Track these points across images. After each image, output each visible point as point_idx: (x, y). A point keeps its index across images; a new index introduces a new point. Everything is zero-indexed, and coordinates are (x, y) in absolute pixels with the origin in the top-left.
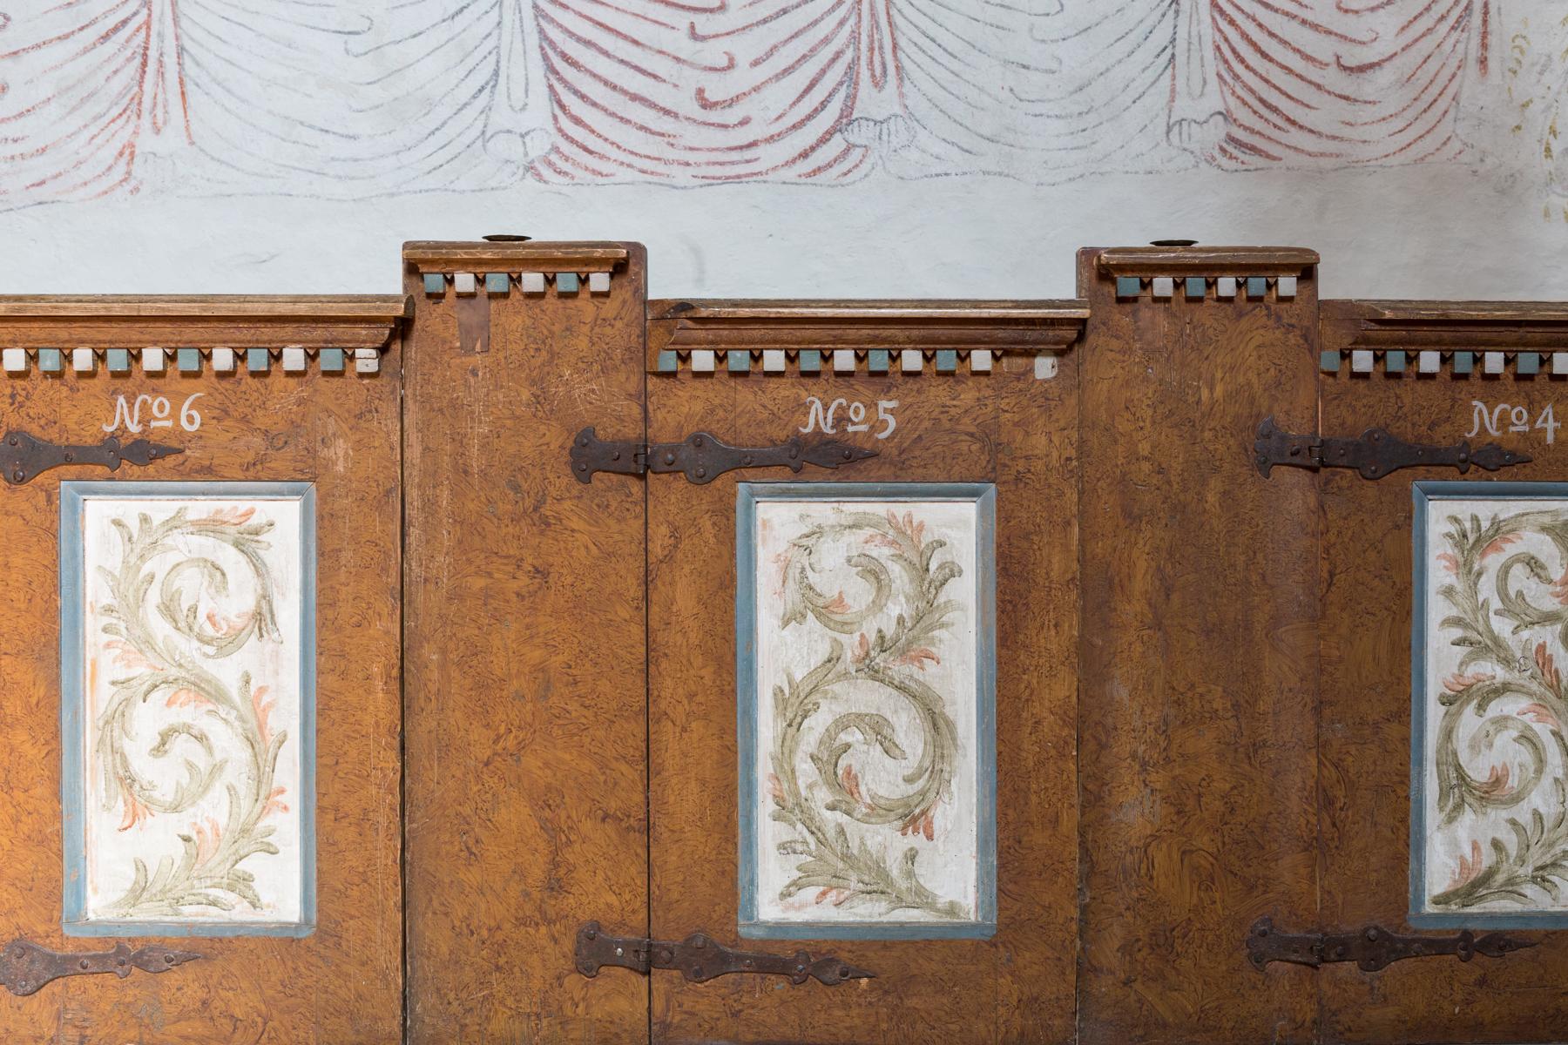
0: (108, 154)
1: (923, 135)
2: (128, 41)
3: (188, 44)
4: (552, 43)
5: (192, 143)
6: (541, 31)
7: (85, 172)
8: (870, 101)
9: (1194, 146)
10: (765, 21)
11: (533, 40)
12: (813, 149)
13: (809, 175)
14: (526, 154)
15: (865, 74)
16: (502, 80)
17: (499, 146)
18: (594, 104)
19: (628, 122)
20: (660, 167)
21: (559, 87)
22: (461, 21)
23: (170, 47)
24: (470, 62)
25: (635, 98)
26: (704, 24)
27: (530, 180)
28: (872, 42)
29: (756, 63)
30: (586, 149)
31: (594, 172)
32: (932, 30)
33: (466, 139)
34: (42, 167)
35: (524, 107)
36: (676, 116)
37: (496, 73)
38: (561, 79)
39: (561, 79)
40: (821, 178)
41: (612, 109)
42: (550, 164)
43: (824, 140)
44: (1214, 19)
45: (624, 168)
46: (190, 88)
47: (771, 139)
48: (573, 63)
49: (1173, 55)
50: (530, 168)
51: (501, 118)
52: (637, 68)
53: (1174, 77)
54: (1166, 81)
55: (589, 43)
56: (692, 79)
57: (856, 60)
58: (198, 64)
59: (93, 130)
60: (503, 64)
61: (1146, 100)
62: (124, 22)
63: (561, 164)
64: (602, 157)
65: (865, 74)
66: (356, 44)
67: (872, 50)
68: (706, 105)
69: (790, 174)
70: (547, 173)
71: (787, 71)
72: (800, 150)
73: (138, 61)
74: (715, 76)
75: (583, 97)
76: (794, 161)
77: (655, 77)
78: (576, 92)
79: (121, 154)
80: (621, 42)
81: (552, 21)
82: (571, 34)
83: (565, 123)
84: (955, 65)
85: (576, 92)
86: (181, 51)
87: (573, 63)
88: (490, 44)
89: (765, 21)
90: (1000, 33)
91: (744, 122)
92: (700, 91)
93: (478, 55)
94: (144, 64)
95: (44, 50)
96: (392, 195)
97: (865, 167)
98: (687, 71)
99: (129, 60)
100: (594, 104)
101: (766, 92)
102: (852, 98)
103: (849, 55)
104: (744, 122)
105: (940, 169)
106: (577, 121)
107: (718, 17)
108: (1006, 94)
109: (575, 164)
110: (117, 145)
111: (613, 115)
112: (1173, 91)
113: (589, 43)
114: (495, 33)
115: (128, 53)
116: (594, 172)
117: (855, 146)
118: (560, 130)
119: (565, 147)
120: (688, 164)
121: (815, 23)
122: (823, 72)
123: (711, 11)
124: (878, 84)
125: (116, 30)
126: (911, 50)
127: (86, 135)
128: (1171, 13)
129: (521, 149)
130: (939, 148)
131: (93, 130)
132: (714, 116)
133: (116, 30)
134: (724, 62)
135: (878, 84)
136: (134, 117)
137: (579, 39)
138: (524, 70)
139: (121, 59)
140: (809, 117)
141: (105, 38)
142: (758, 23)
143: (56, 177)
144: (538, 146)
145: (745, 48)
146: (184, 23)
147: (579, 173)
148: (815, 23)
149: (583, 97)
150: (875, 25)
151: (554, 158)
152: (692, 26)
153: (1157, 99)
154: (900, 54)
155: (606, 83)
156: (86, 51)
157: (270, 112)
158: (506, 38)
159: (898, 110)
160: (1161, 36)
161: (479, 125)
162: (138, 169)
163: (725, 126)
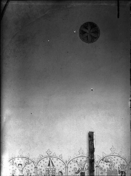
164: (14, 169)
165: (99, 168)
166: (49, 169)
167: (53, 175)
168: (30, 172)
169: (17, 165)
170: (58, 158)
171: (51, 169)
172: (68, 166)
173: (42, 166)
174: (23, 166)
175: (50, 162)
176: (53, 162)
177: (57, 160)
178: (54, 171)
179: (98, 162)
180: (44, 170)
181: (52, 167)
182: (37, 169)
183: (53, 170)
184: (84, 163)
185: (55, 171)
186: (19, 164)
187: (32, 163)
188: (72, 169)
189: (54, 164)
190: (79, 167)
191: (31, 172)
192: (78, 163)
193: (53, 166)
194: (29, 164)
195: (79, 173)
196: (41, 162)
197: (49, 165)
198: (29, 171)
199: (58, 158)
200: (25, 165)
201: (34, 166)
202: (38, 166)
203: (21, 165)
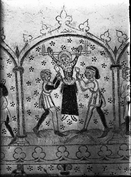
165: (121, 71)
179: (120, 51)
184: (74, 57)
190: (57, 69)
192: (56, 56)
195: (56, 88)
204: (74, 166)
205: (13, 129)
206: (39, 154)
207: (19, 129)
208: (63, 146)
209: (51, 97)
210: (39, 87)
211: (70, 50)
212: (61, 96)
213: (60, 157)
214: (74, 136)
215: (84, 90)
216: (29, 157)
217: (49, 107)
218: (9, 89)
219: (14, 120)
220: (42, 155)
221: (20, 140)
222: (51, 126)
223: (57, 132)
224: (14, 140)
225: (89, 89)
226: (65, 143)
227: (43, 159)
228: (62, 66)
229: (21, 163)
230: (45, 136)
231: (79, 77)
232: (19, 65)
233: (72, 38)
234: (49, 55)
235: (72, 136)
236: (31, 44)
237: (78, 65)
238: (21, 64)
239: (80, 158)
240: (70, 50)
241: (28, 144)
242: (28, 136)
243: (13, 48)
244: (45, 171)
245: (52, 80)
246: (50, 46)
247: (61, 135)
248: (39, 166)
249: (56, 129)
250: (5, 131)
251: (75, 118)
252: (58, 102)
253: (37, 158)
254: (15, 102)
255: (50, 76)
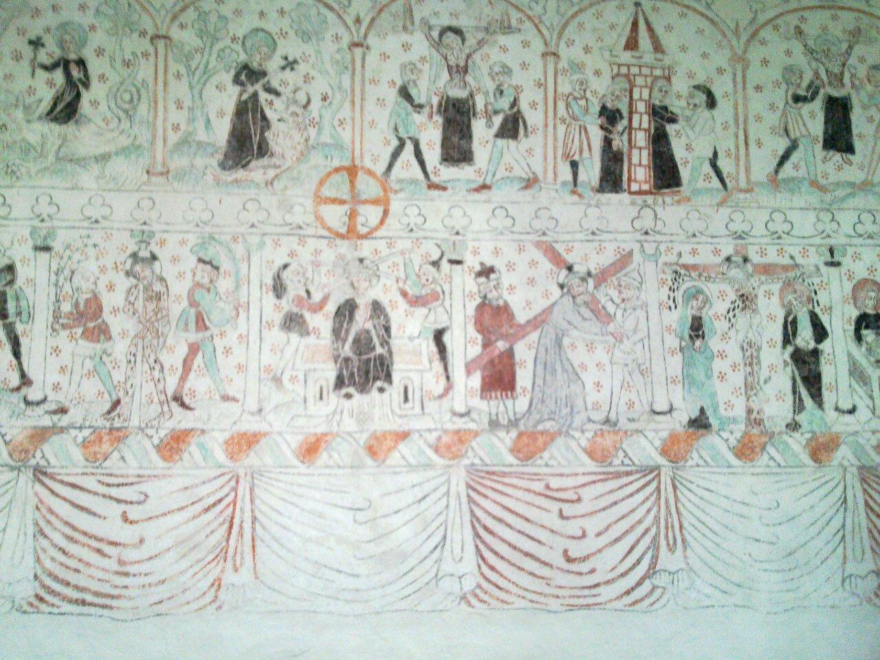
0: (204, 584)
1: (698, 582)
2: (221, 512)
3: (259, 515)
4: (478, 520)
5: (257, 578)
6: (472, 511)
7: (189, 596)
8: (667, 560)
9: (859, 591)
10: (604, 509)
11: (467, 517)
12: (633, 589)
13: (630, 605)
14: (462, 589)
15: (663, 543)
16: (448, 541)
17: (446, 584)
18: (502, 558)
19: (523, 569)
20: (542, 599)
21: (481, 547)
22: (424, 505)
23: (248, 516)
24: (430, 530)
25: (527, 554)
26: (568, 509)
27: (464, 605)
28: (667, 523)
29: (599, 534)
30: (498, 587)
31: (502, 601)
32: (702, 516)
33: (426, 580)
34: (162, 592)
35: (461, 560)
36: (551, 566)
37: (445, 538)
38: (483, 542)
39: (483, 542)
40: (637, 607)
41: (513, 561)
42: (476, 596)
43: (639, 583)
44: (867, 513)
45: (520, 599)
46: (258, 543)
47: (608, 582)
48: (491, 532)
49: (844, 536)
50: (464, 598)
51: (447, 567)
52: (528, 536)
53: (845, 548)
54: (840, 550)
55: (500, 520)
56: (562, 543)
57: (658, 534)
58: (264, 528)
59: (196, 569)
60: (449, 530)
61: (829, 561)
62: (220, 501)
63: (482, 596)
64: (507, 592)
65: (663, 543)
66: (361, 516)
67: (667, 528)
68: (569, 560)
69: (619, 604)
70: (473, 601)
71: (617, 540)
72: (625, 590)
73: (226, 526)
74: (574, 542)
75: (496, 553)
76: (622, 596)
77: (539, 542)
78: (492, 550)
79: (213, 585)
80: (519, 520)
81: (478, 505)
82: (490, 514)
83: (485, 569)
84: (717, 540)
85: (492, 550)
86: (254, 519)
87: (491, 532)
88: (442, 518)
89: (604, 509)
90: (742, 520)
91: (592, 571)
92: (566, 552)
93: (434, 525)
94: (231, 527)
95: (168, 517)
96: (378, 613)
97: (663, 601)
98: (557, 538)
99: (222, 524)
100: (502, 558)
101: (604, 553)
102: (655, 559)
103: (654, 530)
104: (592, 571)
105: (708, 602)
106: (492, 568)
107: (577, 506)
108: (745, 558)
109: (490, 595)
110: (210, 579)
111: (514, 565)
112: (845, 557)
113: (500, 520)
114: (444, 514)
115: (221, 519)
116: (502, 601)
117: (657, 587)
118: (482, 574)
119: (485, 585)
120: (558, 597)
121: (633, 511)
122: (638, 541)
123: (572, 502)
124: (672, 549)
125: (214, 505)
126: (690, 529)
127: (191, 572)
128: (842, 509)
129: (458, 586)
130: (708, 590)
131: (196, 569)
132: (574, 567)
133: (214, 505)
134: (580, 533)
135: (672, 549)
136: (222, 561)
137: (495, 517)
138: (462, 537)
139: (216, 524)
140: (631, 569)
141: (207, 510)
142: (600, 511)
143: (169, 598)
144: (469, 584)
145: (593, 525)
146: (257, 502)
147: (494, 603)
148: (633, 511)
149: (496, 553)
150: (669, 513)
151: (478, 591)
152: (561, 511)
153: (835, 561)
154: (684, 532)
155: (510, 545)
156: (194, 518)
157: (306, 559)
158: (451, 515)
159: (683, 566)
160: (836, 523)
161: (434, 571)
162: (222, 595)
163: (580, 574)
164: (413, 56)
166: (628, 66)
167: (657, 103)
168: (514, 83)
169: (435, 34)
170: (688, 7)
171: (645, 71)
172: (749, 56)
173: (587, 50)
174: (471, 41)
175: (635, 25)
176: (659, 31)
177: (683, 15)
178: (661, 83)
180: (597, 73)
181: (649, 58)
182: (556, 64)
183: (658, 72)
184: (845, 46)
185: (668, 79)
186: (445, 30)
187: (528, 24)
188: (775, 73)
189: (669, 40)
190: (814, 65)
191: (518, 78)
192: (810, 43)
193: (658, 47)
194: (507, 29)
195: (813, 99)
196: (581, 25)
197: (632, 44)
198: (507, 70)
199: (688, 7)
200: (480, 35)
201: (538, 46)
202: (563, 50)
203: (457, 31)
204: (850, 251)
205: (725, 176)
206: (779, 226)
207: (738, 174)
208: (828, 210)
209: (801, 117)
210: (780, 96)
211: (840, 35)
212: (821, 116)
213: (822, 233)
214: (848, 191)
215: (865, 107)
216: (759, 230)
217: (798, 134)
218: (718, 94)
219: (729, 155)
220: (787, 227)
221: (742, 196)
222: (802, 173)
223: (814, 184)
224: (729, 196)
225: (876, 105)
226: (830, 205)
227: (788, 234)
228: (823, 59)
229: (743, 242)
230: (792, 191)
231: (857, 82)
232: (740, 52)
233: (840, 13)
234: (797, 39)
235: (844, 193)
236: (762, 18)
237: (852, 61)
238: (745, 52)
239: (861, 236)
240: (840, 35)
241: (756, 205)
242: (756, 189)
243: (728, 21)
244: (792, 257)
245: (805, 84)
246: (798, 23)
247: (823, 189)
248: (779, 247)
249: (813, 178)
250: (496, 328)
251: (849, 160)
252: (817, 126)
253: (776, 232)
254: (731, 122)
255: (801, 77)
